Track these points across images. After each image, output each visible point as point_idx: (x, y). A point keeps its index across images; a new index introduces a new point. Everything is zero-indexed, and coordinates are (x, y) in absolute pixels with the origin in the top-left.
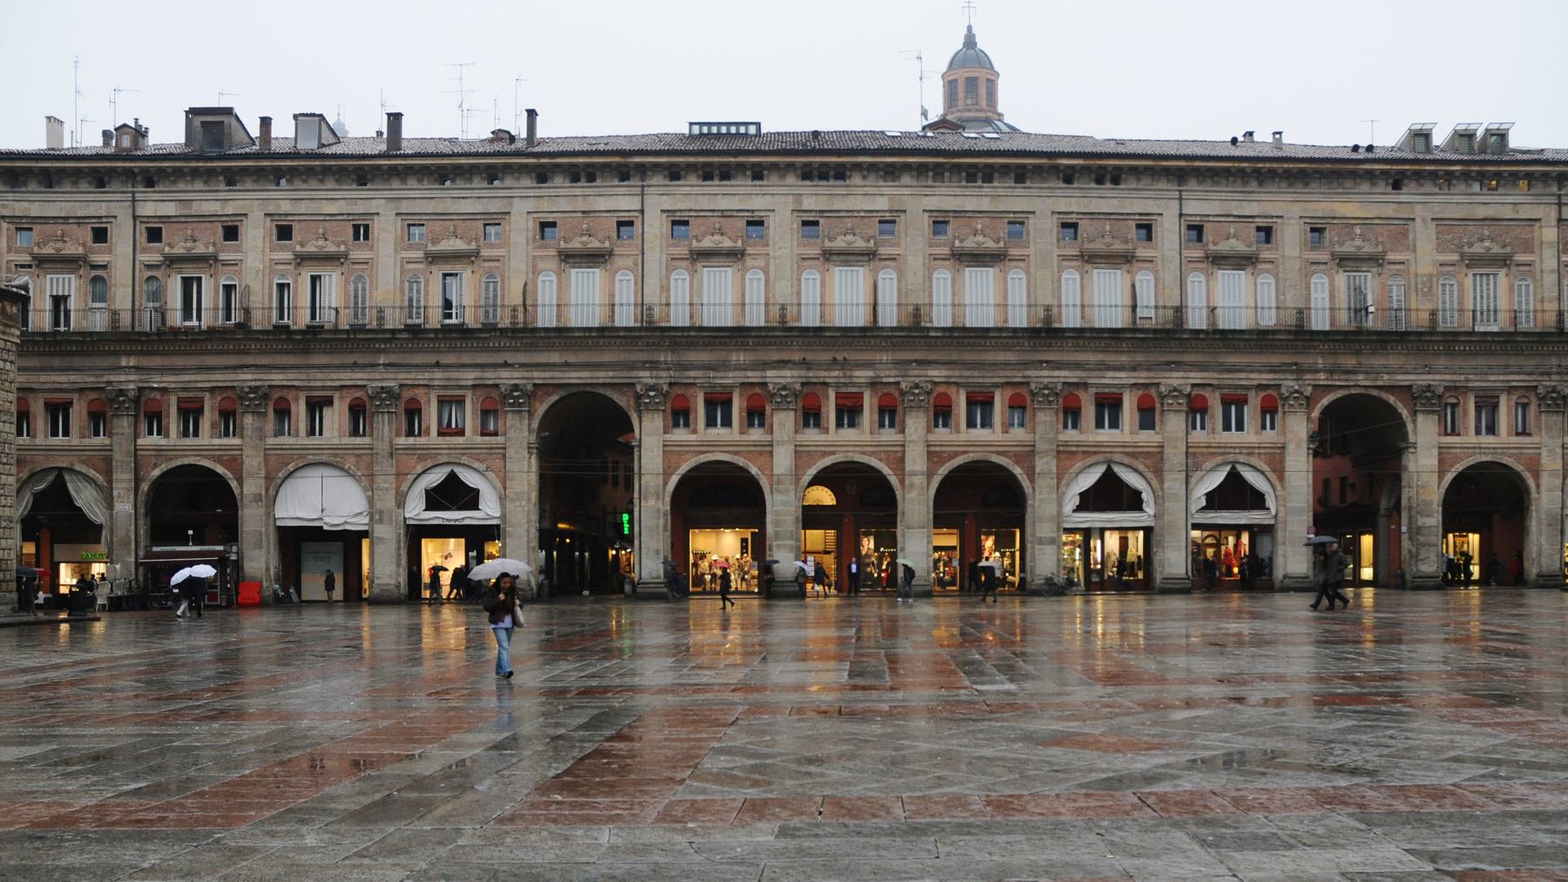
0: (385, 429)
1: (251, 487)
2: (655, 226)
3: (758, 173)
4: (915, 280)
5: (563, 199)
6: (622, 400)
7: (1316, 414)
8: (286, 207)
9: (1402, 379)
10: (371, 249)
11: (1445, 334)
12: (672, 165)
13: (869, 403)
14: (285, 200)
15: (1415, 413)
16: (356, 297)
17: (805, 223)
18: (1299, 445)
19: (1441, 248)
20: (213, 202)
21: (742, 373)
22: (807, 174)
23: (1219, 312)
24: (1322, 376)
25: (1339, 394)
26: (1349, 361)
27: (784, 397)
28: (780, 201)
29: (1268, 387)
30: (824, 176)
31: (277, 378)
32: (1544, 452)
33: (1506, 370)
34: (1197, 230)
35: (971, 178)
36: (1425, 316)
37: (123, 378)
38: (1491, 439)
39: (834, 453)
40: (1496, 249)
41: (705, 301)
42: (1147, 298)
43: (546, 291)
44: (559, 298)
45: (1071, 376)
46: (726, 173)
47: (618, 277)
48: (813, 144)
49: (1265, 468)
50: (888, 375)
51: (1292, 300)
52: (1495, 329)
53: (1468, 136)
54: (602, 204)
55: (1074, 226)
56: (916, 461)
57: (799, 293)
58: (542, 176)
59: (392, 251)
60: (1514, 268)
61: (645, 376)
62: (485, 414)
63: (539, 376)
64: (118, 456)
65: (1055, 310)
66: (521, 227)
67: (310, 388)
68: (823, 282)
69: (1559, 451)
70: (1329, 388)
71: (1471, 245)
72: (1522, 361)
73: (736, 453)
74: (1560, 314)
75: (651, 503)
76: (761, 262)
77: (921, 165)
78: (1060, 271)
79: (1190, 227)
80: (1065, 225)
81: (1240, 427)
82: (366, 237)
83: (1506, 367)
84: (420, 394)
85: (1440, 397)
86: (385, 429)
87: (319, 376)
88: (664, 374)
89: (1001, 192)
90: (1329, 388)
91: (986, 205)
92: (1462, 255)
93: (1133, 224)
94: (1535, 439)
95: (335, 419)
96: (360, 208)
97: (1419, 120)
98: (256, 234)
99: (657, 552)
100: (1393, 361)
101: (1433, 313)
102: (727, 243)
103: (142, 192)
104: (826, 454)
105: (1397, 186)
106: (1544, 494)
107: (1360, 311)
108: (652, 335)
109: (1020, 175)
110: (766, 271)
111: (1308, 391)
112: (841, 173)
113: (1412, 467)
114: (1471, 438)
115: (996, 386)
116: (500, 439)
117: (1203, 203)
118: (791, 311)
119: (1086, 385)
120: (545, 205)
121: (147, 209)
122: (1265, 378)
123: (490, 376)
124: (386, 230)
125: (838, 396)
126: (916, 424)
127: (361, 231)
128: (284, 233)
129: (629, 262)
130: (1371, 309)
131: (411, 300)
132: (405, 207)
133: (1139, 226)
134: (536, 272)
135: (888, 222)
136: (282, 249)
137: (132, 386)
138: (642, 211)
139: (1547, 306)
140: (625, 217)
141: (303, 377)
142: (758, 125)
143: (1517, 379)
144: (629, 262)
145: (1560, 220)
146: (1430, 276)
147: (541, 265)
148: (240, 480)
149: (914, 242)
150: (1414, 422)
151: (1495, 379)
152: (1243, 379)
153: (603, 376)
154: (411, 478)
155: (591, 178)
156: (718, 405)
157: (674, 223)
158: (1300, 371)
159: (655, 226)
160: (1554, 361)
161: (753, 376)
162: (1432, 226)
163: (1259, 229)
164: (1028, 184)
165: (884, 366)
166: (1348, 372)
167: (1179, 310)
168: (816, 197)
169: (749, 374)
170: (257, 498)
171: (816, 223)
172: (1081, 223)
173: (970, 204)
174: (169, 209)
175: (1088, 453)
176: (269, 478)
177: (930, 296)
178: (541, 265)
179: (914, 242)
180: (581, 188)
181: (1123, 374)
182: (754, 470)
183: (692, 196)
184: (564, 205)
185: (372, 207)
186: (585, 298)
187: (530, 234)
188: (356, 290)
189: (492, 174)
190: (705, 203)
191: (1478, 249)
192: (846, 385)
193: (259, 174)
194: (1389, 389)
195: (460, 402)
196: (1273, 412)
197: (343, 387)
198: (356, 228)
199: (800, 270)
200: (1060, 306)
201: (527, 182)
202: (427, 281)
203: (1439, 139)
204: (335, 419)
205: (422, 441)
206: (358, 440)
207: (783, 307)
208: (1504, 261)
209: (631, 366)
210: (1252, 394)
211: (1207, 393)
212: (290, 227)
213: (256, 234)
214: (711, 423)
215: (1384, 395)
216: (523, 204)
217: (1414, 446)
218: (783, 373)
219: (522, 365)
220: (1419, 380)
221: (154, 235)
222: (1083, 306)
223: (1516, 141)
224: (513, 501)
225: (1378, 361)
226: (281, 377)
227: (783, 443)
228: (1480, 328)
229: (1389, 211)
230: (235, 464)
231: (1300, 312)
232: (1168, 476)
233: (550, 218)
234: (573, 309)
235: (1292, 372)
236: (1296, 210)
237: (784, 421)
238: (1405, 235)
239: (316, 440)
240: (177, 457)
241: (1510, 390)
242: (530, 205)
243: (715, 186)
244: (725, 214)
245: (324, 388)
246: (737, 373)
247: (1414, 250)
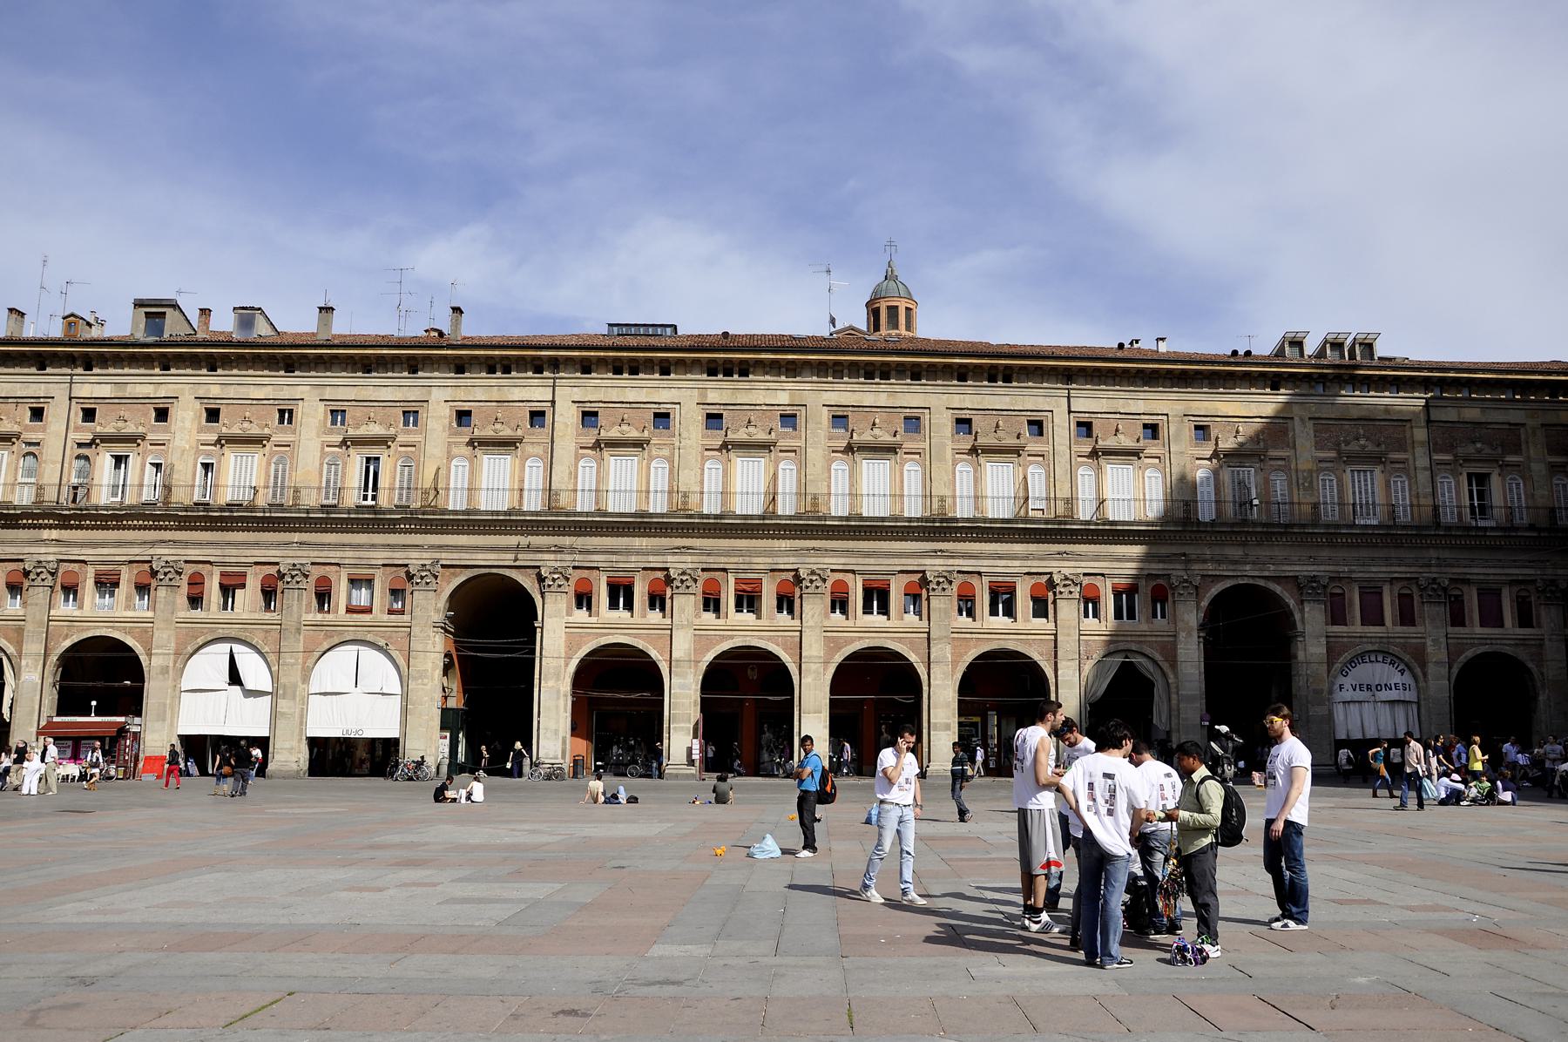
0: (298, 605)
2: (566, 417)
3: (665, 369)
4: (814, 470)
5: (478, 389)
6: (528, 582)
7: (1205, 603)
8: (215, 391)
9: (1289, 570)
10: (294, 432)
11: (1328, 526)
12: (583, 359)
13: (127, 577)
14: (215, 385)
15: (1302, 602)
16: (276, 477)
17: (709, 416)
18: (1189, 634)
19: (1319, 446)
20: (146, 385)
21: (644, 558)
22: (712, 370)
23: (1108, 504)
24: (1210, 566)
25: (1228, 584)
26: (1235, 552)
28: (686, 395)
29: (1157, 576)
31: (194, 553)
32: (1429, 643)
33: (1387, 561)
34: (1086, 427)
35: (869, 375)
36: (1307, 509)
37: (43, 550)
39: (732, 637)
40: (1370, 447)
41: (611, 488)
42: (1037, 488)
43: (458, 475)
44: (470, 483)
46: (635, 368)
47: (528, 463)
48: (724, 342)
49: (1158, 657)
51: (1063, 491)
52: (1375, 522)
53: (1337, 345)
54: (517, 394)
55: (968, 422)
56: (813, 647)
57: (702, 482)
58: (460, 367)
59: (314, 434)
60: (1389, 466)
62: (396, 593)
64: (29, 626)
65: (949, 501)
66: (438, 415)
67: (224, 564)
68: (725, 473)
69: (1443, 640)
70: (1217, 578)
71: (1347, 443)
72: (1402, 553)
73: (636, 636)
74: (1436, 508)
75: (551, 683)
76: (666, 452)
77: (821, 363)
78: (955, 464)
79: (1079, 424)
80: (959, 421)
81: (1131, 616)
82: (290, 422)
83: (1387, 559)
85: (1325, 587)
86: (298, 605)
87: (234, 552)
88: (568, 557)
89: (898, 388)
90: (1217, 578)
91: (882, 400)
92: (1339, 452)
93: (1025, 420)
94: (1420, 629)
95: (248, 599)
96: (286, 393)
97: (1294, 327)
98: (187, 416)
99: (556, 732)
100: (1278, 553)
101: (1316, 506)
102: (634, 434)
104: (724, 638)
106: (1431, 682)
107: (1245, 504)
108: (557, 523)
109: (916, 373)
110: (670, 460)
111: (1197, 581)
112: (744, 369)
113: (1301, 655)
114: (1357, 628)
115: (249, 565)
116: (406, 617)
117: (1090, 400)
118: (693, 500)
120: (461, 394)
121: (84, 390)
123: (399, 557)
124: (312, 415)
127: (286, 415)
128: (213, 415)
129: (539, 450)
130: (1256, 502)
131: (328, 481)
133: (1030, 423)
134: (450, 457)
135: (789, 419)
136: (209, 431)
137: (51, 558)
138: (553, 402)
139: (1422, 501)
140: (537, 407)
141: (219, 552)
142: (675, 327)
143: (1399, 571)
144: (539, 450)
146: (1310, 471)
147: (455, 450)
148: (150, 655)
150: (1302, 611)
151: (1378, 571)
152: (722, 562)
153: (508, 559)
154: (317, 654)
155: (507, 370)
157: (585, 414)
158: (1188, 560)
159: (566, 417)
160: (1433, 553)
162: (1310, 424)
163: (1145, 426)
164: (751, 377)
165: (785, 553)
166: (1236, 562)
167: (1070, 502)
168: (720, 391)
169: (651, 558)
170: (164, 670)
171: (720, 416)
172: (725, 414)
173: (868, 400)
174: (105, 391)
177: (829, 487)
178: (455, 450)
179: (818, 434)
180: (498, 380)
181: (1017, 563)
183: (602, 388)
184: (480, 394)
185: (297, 393)
186: (495, 483)
187: (447, 421)
188: (277, 471)
189: (413, 366)
190: (614, 395)
191: (1354, 447)
192: (745, 571)
193: (194, 361)
194: (1277, 579)
195: (369, 582)
196: (1164, 602)
197: (257, 563)
198: (282, 412)
199: (704, 460)
200: (954, 497)
202: (345, 464)
203: (1310, 347)
204: (248, 599)
205: (330, 617)
206: (268, 616)
207: (685, 495)
208: (1378, 459)
210: (124, 570)
211: (1098, 581)
212: (218, 410)
213: (187, 416)
216: (440, 394)
217: (1303, 634)
218: (683, 558)
219: (432, 547)
220: (1304, 570)
221: (89, 415)
222: (976, 497)
223: (1381, 350)
224: (415, 679)
225: (1264, 552)
226: (197, 552)
227: (683, 627)
228: (1360, 521)
231: (1187, 503)
232: (287, 659)
233: (466, 407)
234: (483, 493)
235: (1181, 562)
237: (686, 605)
238: (1285, 432)
239: (228, 614)
240: (88, 628)
242: (448, 394)
243: (625, 379)
245: (238, 564)
246: (640, 558)
247: (1294, 447)
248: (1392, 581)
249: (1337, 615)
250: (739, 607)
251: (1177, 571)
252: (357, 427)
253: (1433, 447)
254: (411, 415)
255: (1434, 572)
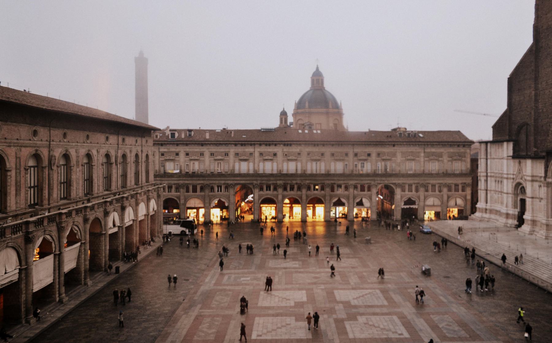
1: (182, 201)
2: (257, 154)
6: (251, 186)
8: (188, 150)
9: (394, 182)
20: (173, 149)
26: (384, 179)
27: (280, 186)
30: (288, 145)
31: (187, 182)
38: (410, 193)
45: (333, 182)
50: (299, 182)
54: (247, 150)
61: (255, 182)
63: (236, 182)
84: (214, 185)
90: (380, 184)
91: (317, 150)
96: (202, 150)
100: (392, 179)
102: (270, 158)
103: (160, 147)
105: (394, 146)
107: (386, 170)
114: (407, 192)
119: (335, 184)
120: (236, 150)
122: (369, 182)
123: (227, 182)
125: (290, 186)
126: (304, 191)
132: (210, 150)
135: (299, 154)
143: (416, 182)
145: (424, 152)
149: (304, 158)
151: (411, 182)
153: (248, 182)
156: (268, 188)
158: (374, 180)
159: (257, 154)
161: (275, 182)
168: (286, 149)
174: (166, 150)
175: (335, 196)
176: (185, 201)
180: (243, 147)
182: (275, 199)
191: (409, 158)
194: (392, 184)
201: (233, 146)
205: (214, 194)
209: (253, 180)
214: (267, 190)
215: (391, 185)
229: (392, 150)
230: (179, 198)
236: (375, 150)
237: (280, 190)
241: (415, 184)
243: (268, 147)
244: (269, 152)
248: (415, 184)
249: (403, 191)
250: (290, 190)
251: (373, 183)
252: (216, 156)
253: (425, 157)
254: (227, 154)
255: (423, 182)
